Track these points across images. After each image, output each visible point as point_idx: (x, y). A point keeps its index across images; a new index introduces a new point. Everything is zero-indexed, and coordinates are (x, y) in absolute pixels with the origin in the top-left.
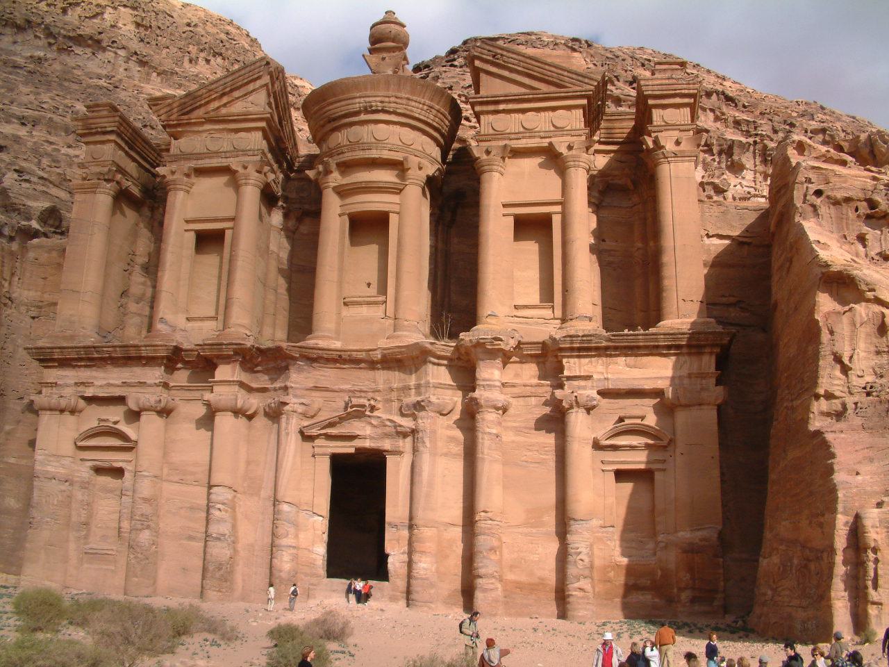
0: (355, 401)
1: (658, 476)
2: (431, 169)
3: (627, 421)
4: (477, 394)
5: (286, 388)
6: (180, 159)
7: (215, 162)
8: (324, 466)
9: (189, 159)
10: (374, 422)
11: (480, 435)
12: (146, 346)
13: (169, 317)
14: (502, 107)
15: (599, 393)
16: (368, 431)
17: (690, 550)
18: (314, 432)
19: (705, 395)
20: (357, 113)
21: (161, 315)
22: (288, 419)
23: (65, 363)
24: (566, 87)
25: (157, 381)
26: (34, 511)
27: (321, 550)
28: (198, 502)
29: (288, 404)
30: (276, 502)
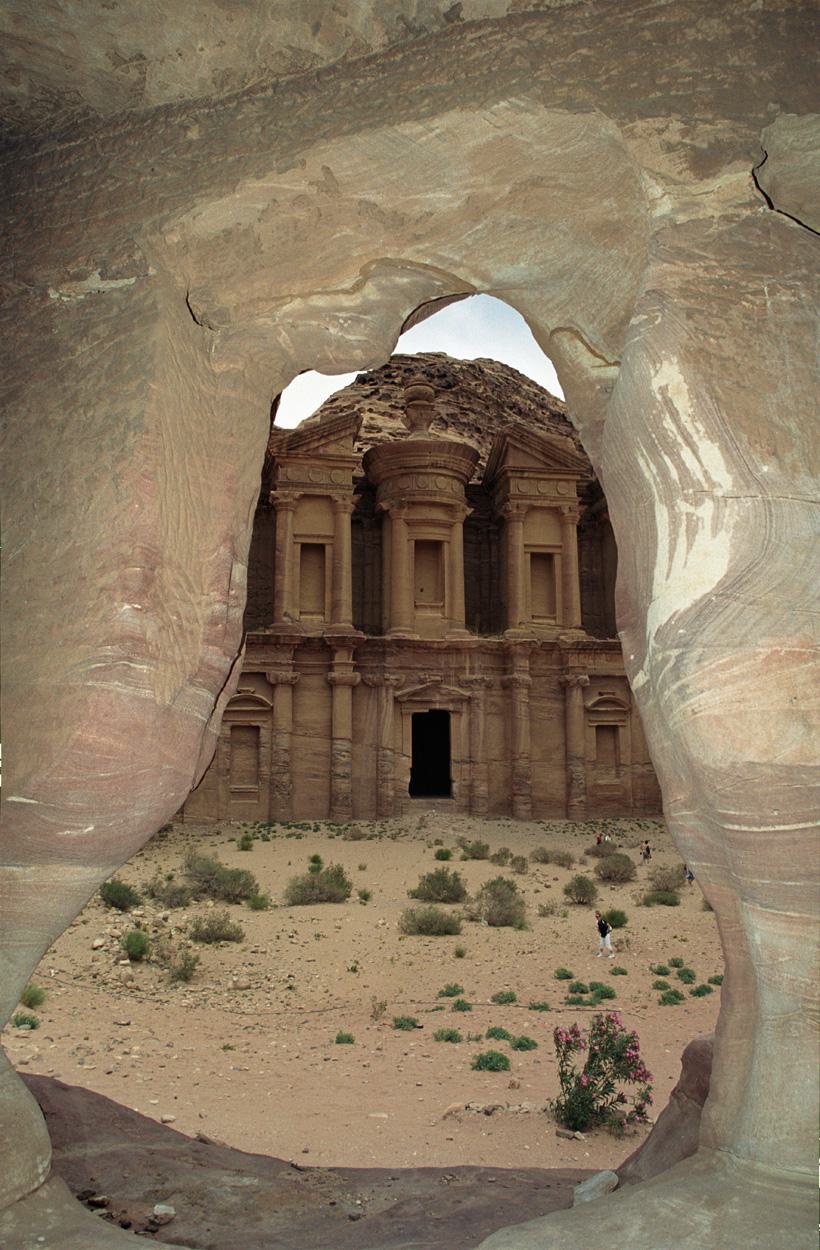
0: (433, 678)
1: (621, 730)
2: (470, 511)
5: (384, 667)
6: (288, 486)
7: (317, 491)
8: (408, 723)
9: (296, 486)
10: (443, 692)
11: (518, 703)
12: (285, 636)
13: (290, 612)
14: (526, 475)
15: (590, 677)
16: (438, 698)
18: (405, 699)
20: (426, 467)
21: (284, 610)
22: (387, 690)
25: (290, 662)
27: (409, 780)
28: (319, 749)
30: (378, 748)
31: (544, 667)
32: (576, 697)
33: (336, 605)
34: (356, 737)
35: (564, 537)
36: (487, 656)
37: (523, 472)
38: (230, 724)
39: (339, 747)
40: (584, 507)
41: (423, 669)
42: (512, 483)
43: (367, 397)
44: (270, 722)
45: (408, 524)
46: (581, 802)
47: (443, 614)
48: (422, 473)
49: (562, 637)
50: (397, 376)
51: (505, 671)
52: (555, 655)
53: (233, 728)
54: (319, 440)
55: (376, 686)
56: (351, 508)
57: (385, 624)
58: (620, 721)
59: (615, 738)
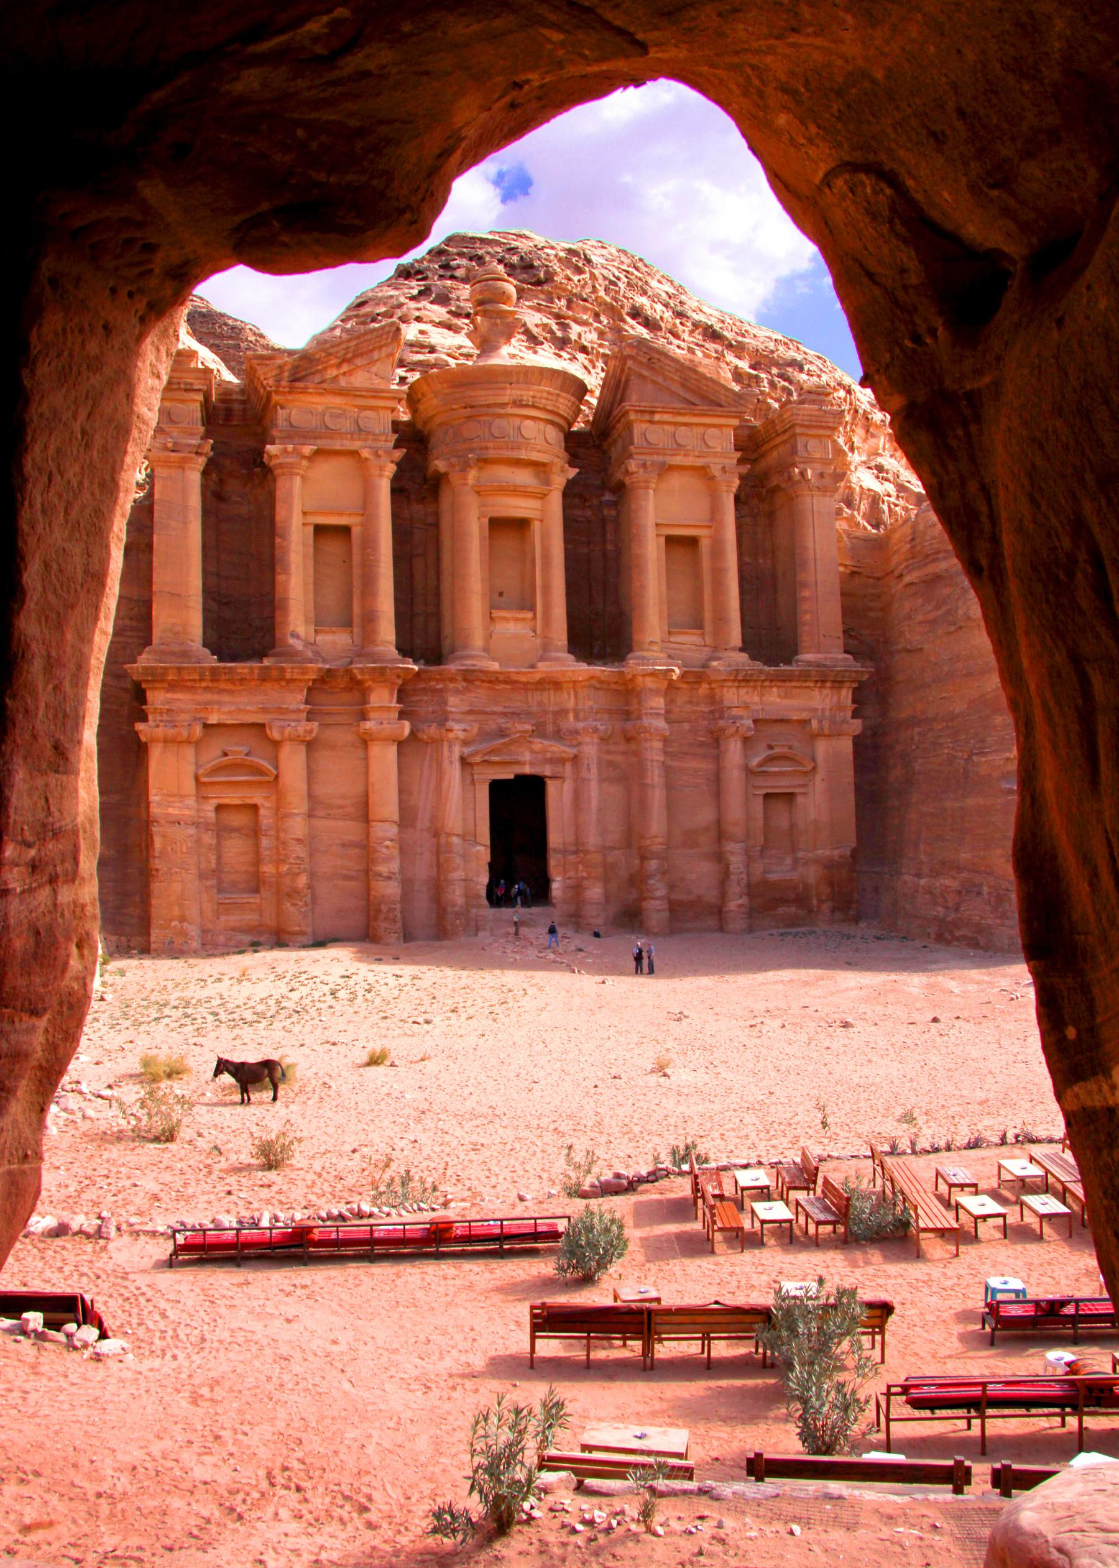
1: (800, 800)
2: (572, 473)
3: (777, 750)
4: (646, 721)
7: (337, 445)
13: (301, 630)
14: (657, 417)
15: (755, 721)
16: (527, 757)
17: (830, 865)
18: (478, 759)
19: (845, 726)
20: (503, 405)
21: (291, 628)
23: (173, 686)
24: (721, 406)
26: (157, 861)
27: (485, 879)
28: (350, 837)
29: (451, 730)
31: (688, 708)
32: (734, 751)
33: (370, 618)
34: (407, 817)
35: (715, 511)
36: (601, 693)
37: (653, 413)
38: (215, 802)
39: (380, 834)
40: (745, 469)
41: (504, 714)
42: (638, 429)
43: (412, 298)
44: (274, 797)
45: (478, 493)
46: (741, 906)
47: (535, 631)
48: (500, 416)
49: (715, 664)
50: (459, 267)
51: (627, 715)
52: (704, 689)
53: (219, 808)
54: (339, 366)
55: (437, 742)
56: (391, 469)
57: (446, 645)
58: (799, 786)
59: (790, 812)
